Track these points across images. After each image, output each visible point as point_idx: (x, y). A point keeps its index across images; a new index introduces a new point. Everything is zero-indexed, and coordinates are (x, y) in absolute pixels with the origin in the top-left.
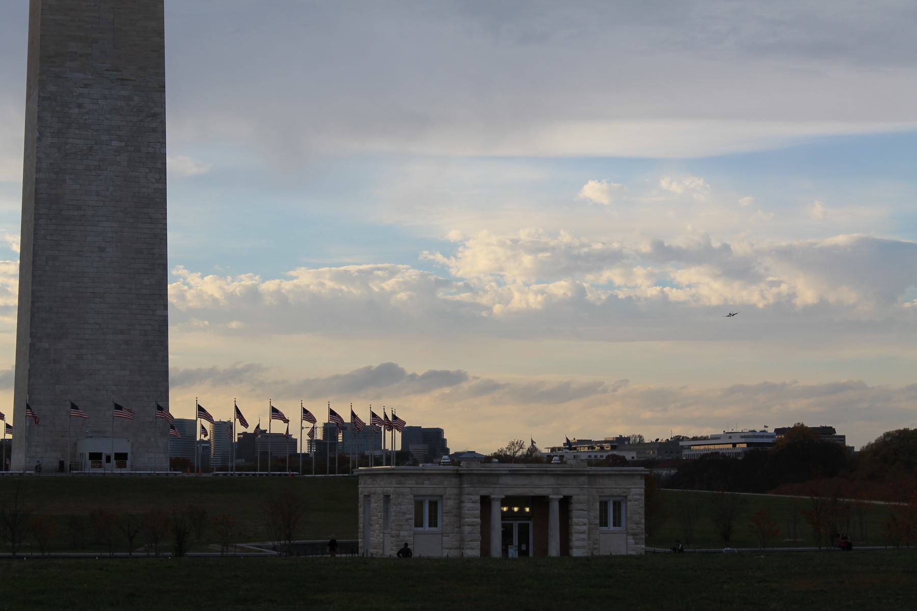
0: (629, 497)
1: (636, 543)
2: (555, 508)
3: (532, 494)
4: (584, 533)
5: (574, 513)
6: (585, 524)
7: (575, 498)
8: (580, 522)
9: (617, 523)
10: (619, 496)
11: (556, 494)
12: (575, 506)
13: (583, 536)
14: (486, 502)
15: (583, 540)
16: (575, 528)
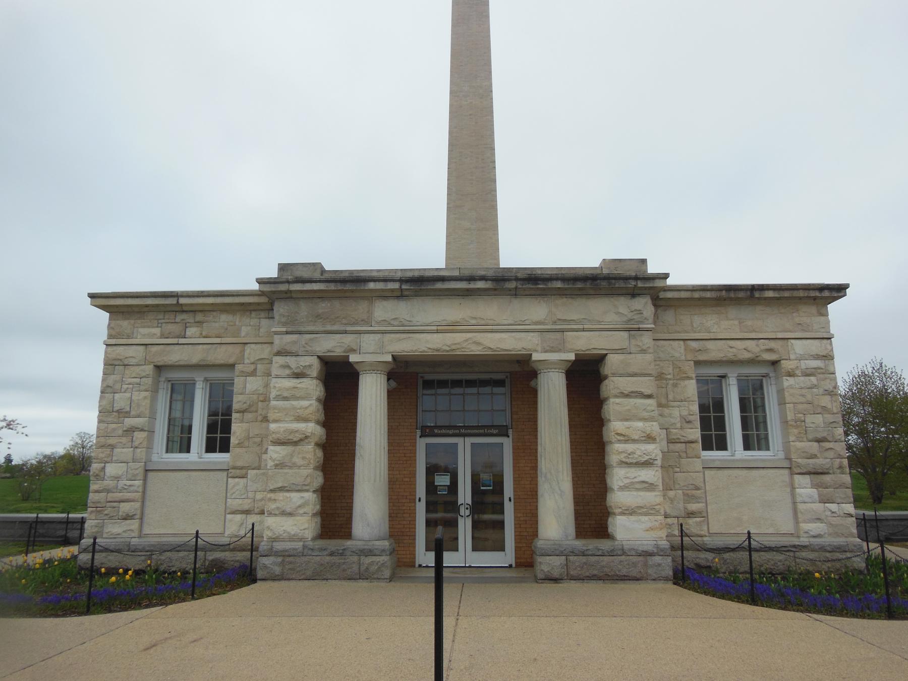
0: (786, 365)
1: (824, 501)
2: (553, 392)
3: (476, 350)
4: (648, 464)
5: (614, 407)
6: (650, 438)
7: (613, 362)
8: (632, 424)
9: (754, 438)
10: (753, 362)
11: (552, 350)
12: (612, 386)
13: (647, 475)
14: (339, 380)
15: (649, 487)
16: (616, 451)
